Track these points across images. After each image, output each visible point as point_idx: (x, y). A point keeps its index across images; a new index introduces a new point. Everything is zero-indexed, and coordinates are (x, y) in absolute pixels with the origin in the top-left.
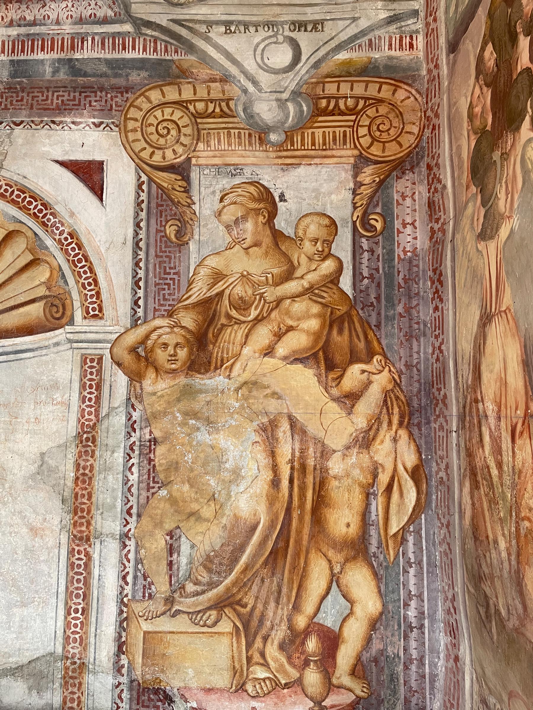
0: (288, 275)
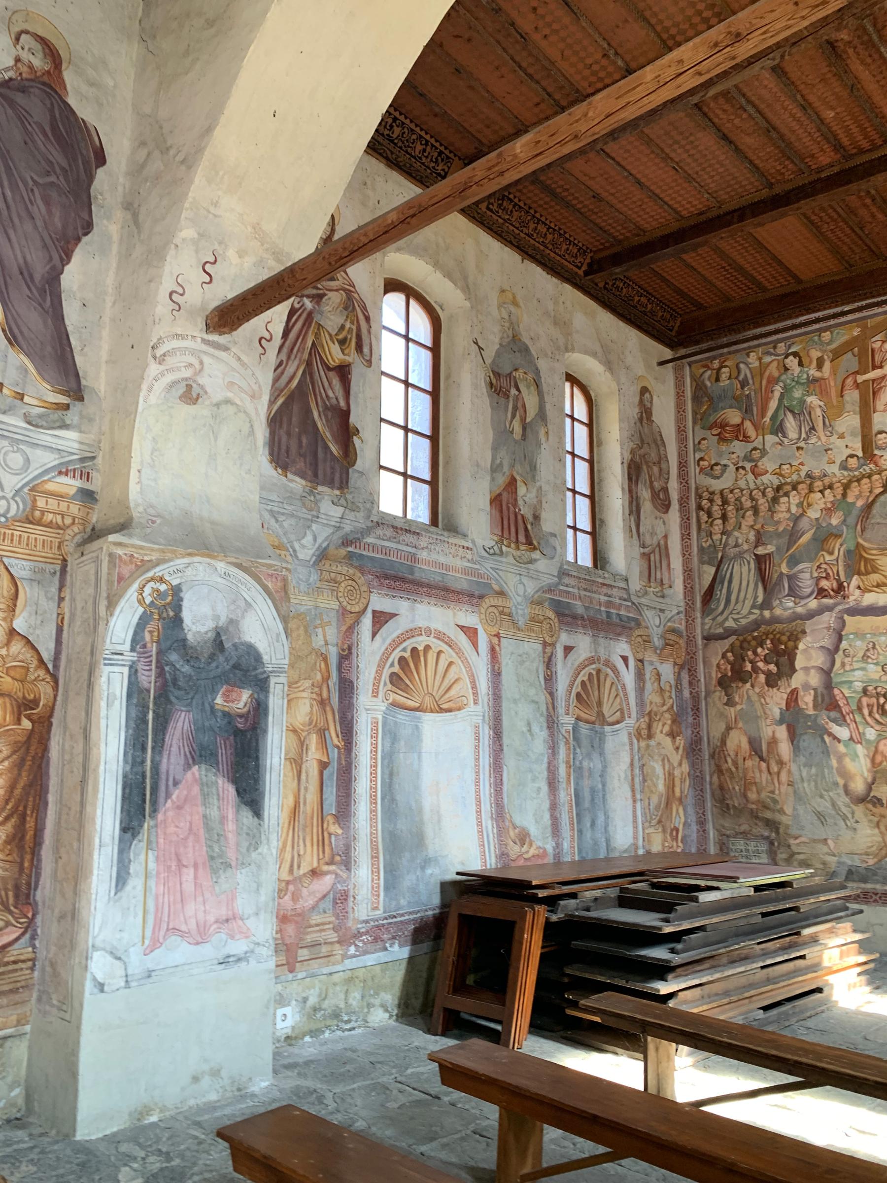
0: (663, 705)
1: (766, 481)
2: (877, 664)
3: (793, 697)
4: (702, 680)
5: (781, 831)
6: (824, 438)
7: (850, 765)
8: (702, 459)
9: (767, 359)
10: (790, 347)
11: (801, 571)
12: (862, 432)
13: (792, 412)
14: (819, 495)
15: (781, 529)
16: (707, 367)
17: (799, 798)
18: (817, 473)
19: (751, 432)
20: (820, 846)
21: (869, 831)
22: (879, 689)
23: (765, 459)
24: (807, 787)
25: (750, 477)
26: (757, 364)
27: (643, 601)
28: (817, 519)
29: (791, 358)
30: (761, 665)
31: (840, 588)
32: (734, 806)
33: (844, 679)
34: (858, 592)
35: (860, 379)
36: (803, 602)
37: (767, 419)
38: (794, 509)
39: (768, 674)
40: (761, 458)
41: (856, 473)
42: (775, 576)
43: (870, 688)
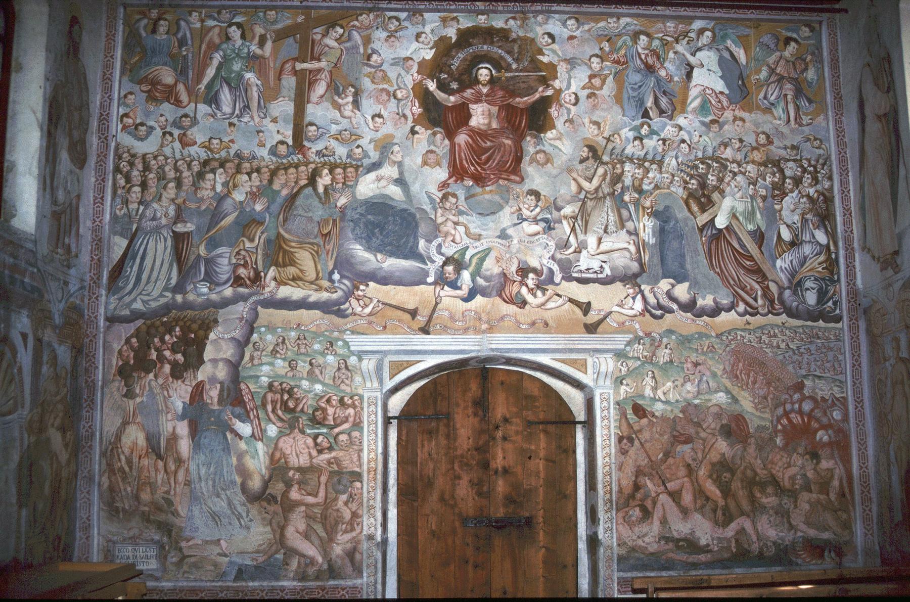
1: (193, 153)
2: (284, 359)
3: (198, 391)
4: (101, 367)
5: (174, 533)
6: (257, 119)
7: (251, 464)
8: (126, 115)
9: (210, 23)
10: (234, 16)
11: (220, 256)
12: (295, 120)
13: (229, 85)
14: (246, 177)
15: (204, 207)
16: (144, 15)
17: (194, 498)
18: (246, 152)
19: (184, 97)
20: (212, 547)
21: (261, 529)
22: (284, 385)
23: (195, 129)
24: (204, 488)
25: (177, 145)
26: (198, 25)
27: (50, 269)
28: (241, 203)
29: (234, 28)
30: (167, 353)
31: (257, 279)
32: (124, 509)
33: (252, 373)
34: (273, 284)
35: (299, 66)
36: (218, 289)
37: (202, 86)
38: (219, 188)
39: (174, 365)
40: (191, 127)
41: (285, 161)
42: (192, 258)
43: (276, 384)
